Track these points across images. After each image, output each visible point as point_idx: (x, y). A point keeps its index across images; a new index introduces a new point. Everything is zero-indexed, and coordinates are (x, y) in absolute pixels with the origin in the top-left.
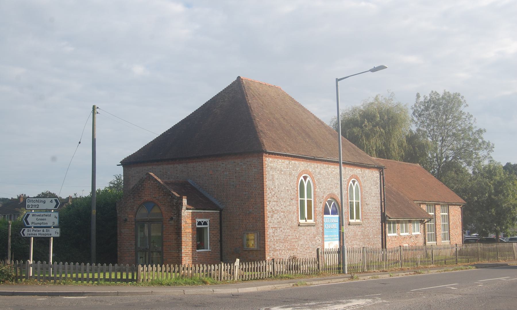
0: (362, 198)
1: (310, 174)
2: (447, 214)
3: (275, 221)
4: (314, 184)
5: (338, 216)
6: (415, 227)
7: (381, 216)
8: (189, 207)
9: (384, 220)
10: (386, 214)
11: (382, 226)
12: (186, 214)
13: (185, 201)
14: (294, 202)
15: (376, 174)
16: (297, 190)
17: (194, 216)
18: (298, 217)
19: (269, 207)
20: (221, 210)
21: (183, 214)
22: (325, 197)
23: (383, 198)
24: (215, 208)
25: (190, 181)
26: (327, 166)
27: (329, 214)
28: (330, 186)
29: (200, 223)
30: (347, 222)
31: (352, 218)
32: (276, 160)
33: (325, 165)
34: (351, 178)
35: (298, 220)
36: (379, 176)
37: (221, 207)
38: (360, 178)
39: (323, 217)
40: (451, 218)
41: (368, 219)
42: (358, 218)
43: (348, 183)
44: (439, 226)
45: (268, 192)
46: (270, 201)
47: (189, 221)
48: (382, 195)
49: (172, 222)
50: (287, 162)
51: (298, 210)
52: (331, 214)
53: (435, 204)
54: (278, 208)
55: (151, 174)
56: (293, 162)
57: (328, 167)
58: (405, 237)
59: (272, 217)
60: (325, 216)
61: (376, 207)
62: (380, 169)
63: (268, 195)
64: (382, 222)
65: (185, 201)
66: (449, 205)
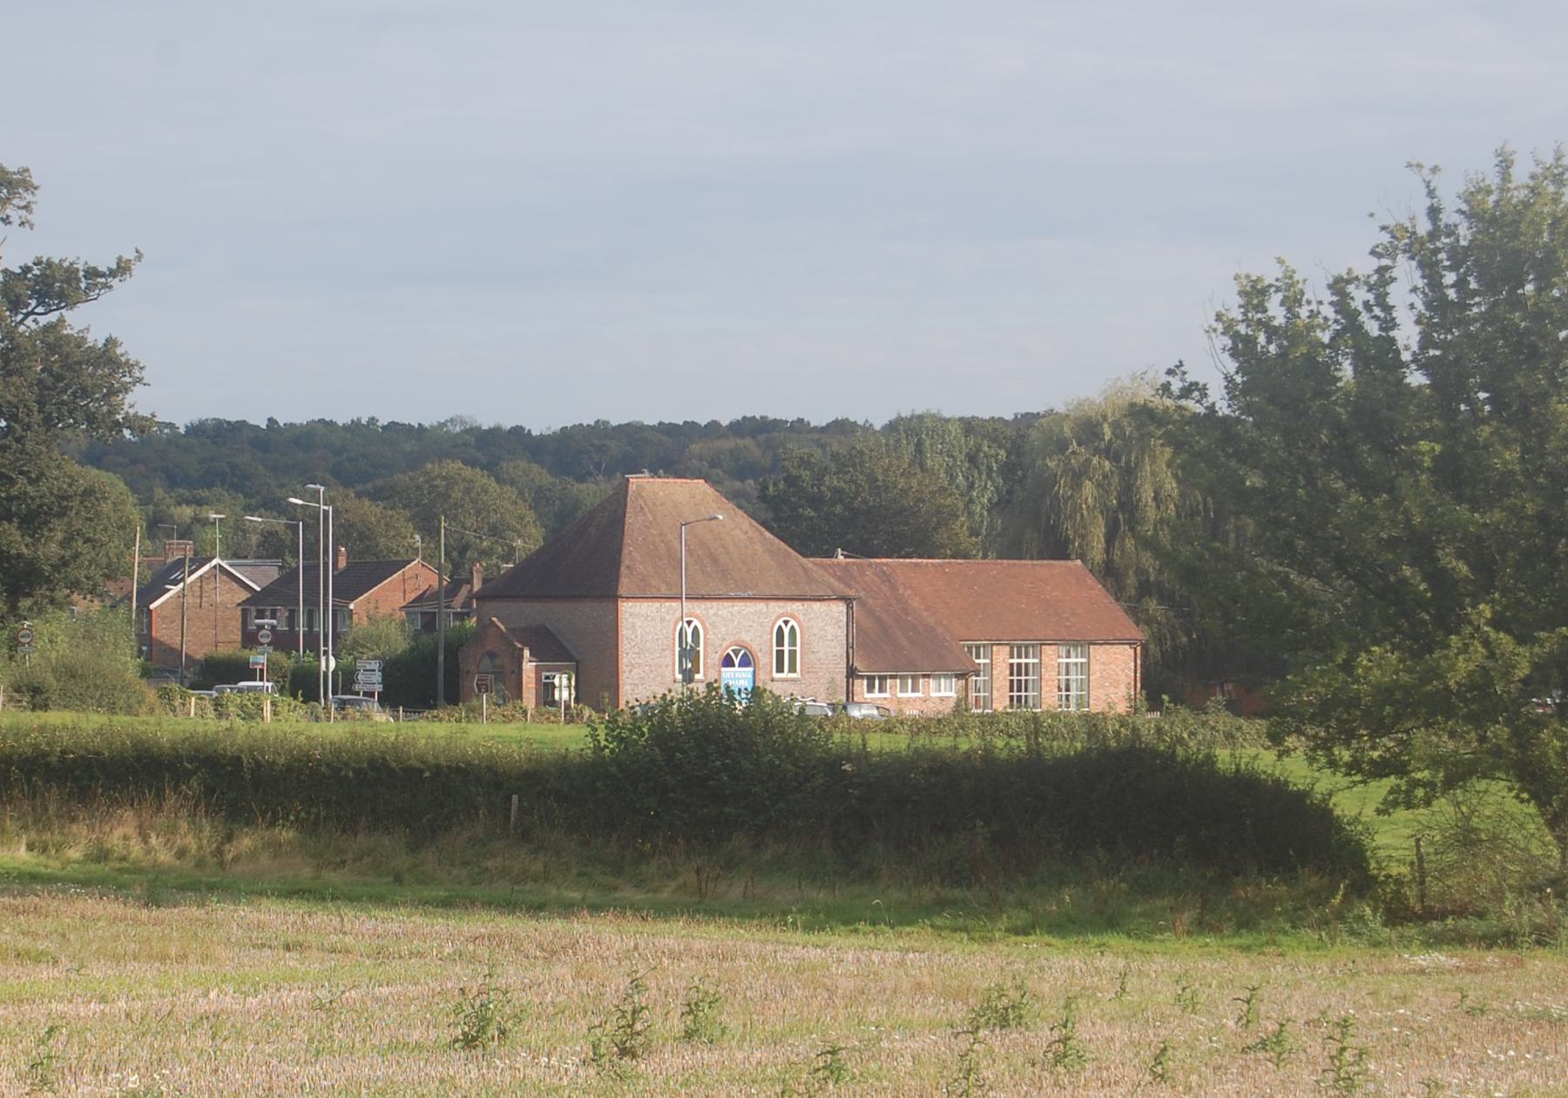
0: (802, 643)
1: (697, 617)
2: (1084, 660)
3: (636, 677)
4: (705, 628)
5: (751, 669)
6: (940, 685)
7: (847, 668)
8: (533, 659)
9: (851, 673)
10: (855, 664)
11: (848, 682)
12: (529, 667)
13: (527, 653)
14: (667, 652)
15: (839, 609)
16: (674, 639)
17: (538, 670)
18: (674, 671)
19: (625, 661)
20: (577, 662)
21: (524, 667)
22: (724, 645)
23: (851, 641)
24: (570, 658)
25: (548, 626)
26: (730, 604)
27: (734, 666)
28: (734, 631)
29: (547, 678)
30: (768, 677)
31: (780, 669)
32: (638, 604)
33: (726, 604)
34: (779, 617)
35: (674, 675)
36: (845, 611)
37: (578, 658)
38: (801, 617)
39: (720, 671)
40: (1094, 667)
41: (816, 672)
42: (792, 669)
43: (774, 624)
44: (1050, 683)
45: (625, 642)
46: (627, 654)
47: (533, 675)
48: (851, 636)
49: (513, 676)
50: (657, 605)
51: (674, 664)
52: (740, 666)
53: (992, 645)
54: (640, 661)
55: (494, 619)
56: (667, 604)
57: (733, 606)
58: (908, 700)
59: (630, 672)
60: (723, 669)
61: (835, 656)
62: (847, 600)
63: (625, 646)
64: (847, 677)
65: (527, 653)
66: (1090, 644)
